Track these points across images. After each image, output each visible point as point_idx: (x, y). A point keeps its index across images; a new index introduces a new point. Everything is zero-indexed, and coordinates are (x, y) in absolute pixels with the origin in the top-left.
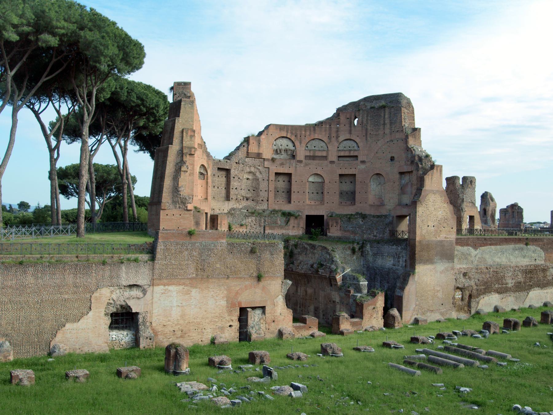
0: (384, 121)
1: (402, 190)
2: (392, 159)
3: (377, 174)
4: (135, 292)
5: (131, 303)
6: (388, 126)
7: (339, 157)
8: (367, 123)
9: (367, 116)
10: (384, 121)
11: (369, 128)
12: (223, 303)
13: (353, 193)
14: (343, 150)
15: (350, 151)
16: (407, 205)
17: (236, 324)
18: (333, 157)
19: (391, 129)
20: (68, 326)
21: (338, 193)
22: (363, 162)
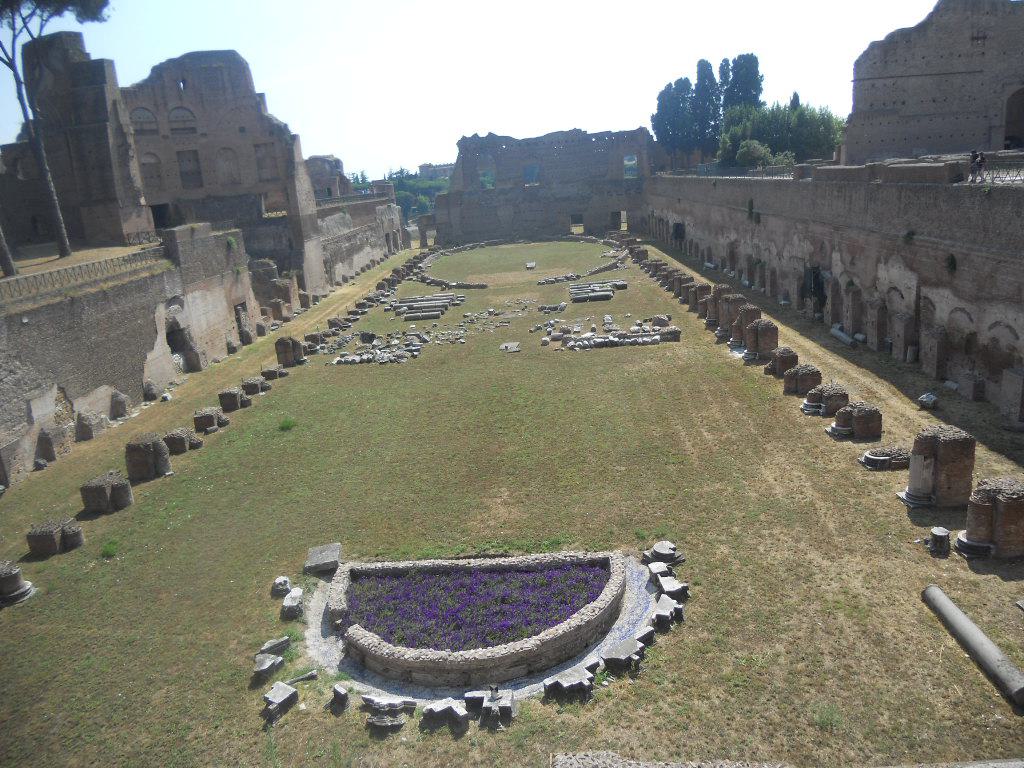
2: (242, 130)
4: (176, 307)
5: (179, 318)
7: (172, 130)
12: (225, 303)
13: (200, 173)
14: (175, 121)
15: (184, 121)
16: (268, 180)
17: (235, 325)
18: (165, 130)
20: (150, 356)
21: (178, 174)
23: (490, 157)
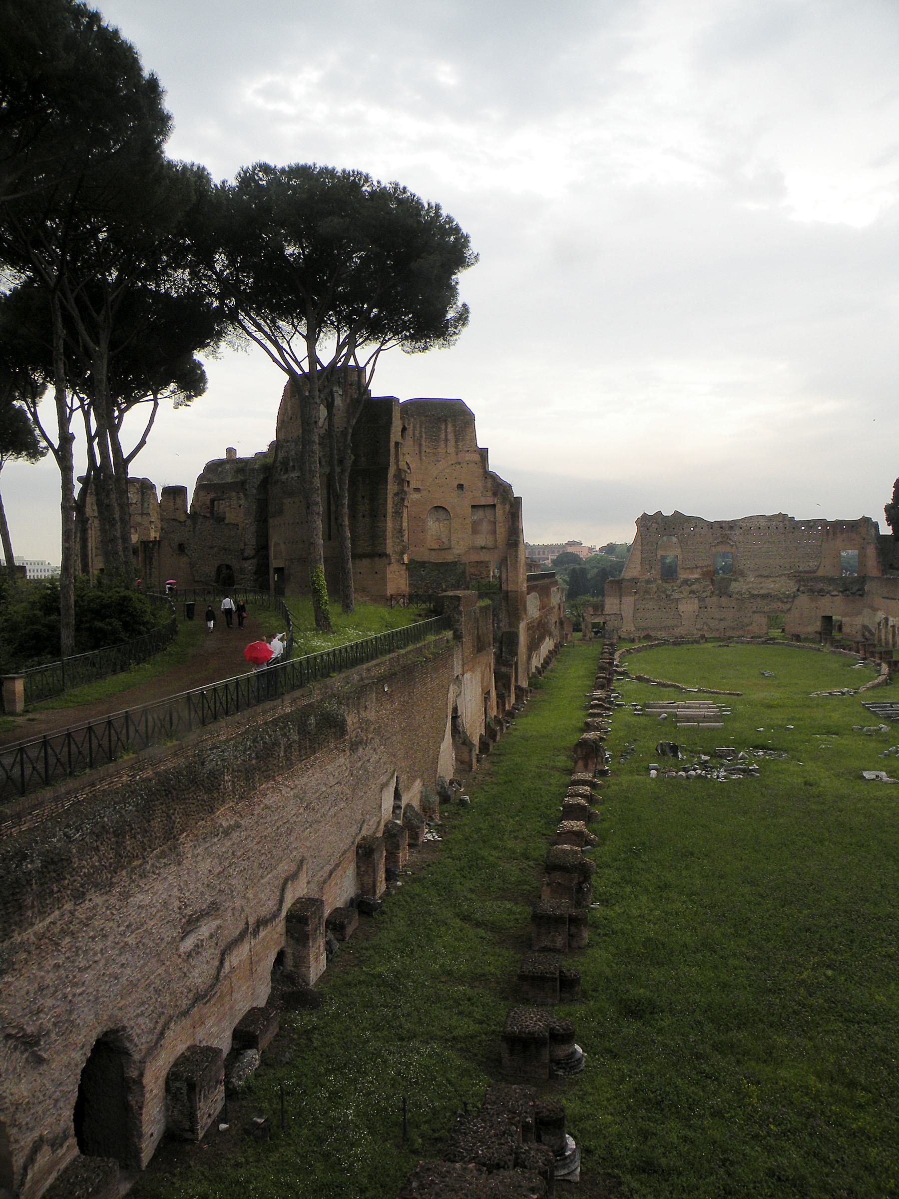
0: (446, 436)
1: (475, 531)
2: (460, 487)
3: (436, 507)
6: (452, 443)
8: (421, 436)
9: (421, 427)
10: (446, 436)
11: (424, 443)
16: (482, 548)
19: (457, 446)
22: (417, 490)
23: (674, 539)
